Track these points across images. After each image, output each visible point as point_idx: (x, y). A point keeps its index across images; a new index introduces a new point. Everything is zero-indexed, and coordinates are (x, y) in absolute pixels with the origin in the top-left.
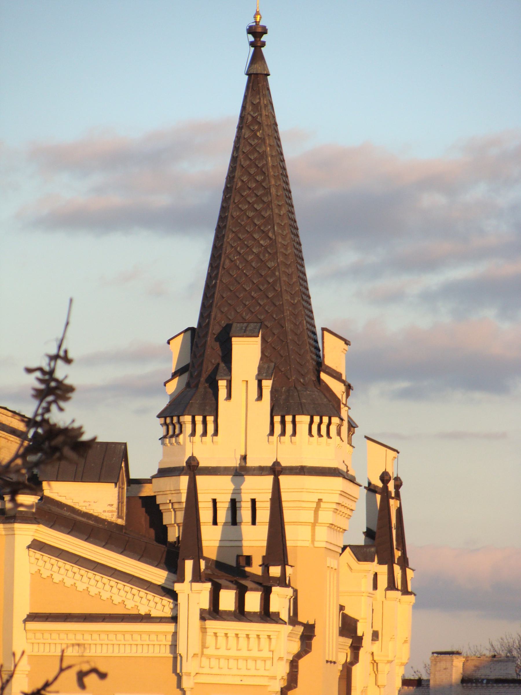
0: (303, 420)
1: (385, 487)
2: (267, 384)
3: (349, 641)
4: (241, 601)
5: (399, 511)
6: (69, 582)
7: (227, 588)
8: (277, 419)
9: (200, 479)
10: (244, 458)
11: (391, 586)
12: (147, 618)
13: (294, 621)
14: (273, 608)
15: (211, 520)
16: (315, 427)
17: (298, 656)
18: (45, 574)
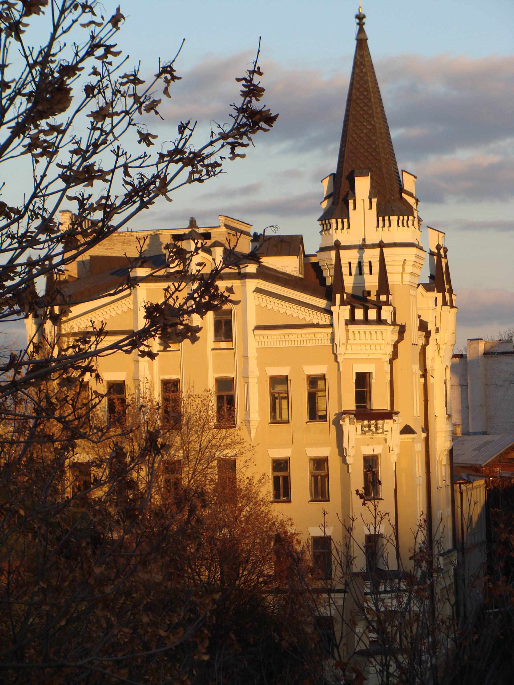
0: (394, 218)
1: (439, 252)
2: (374, 201)
3: (424, 334)
4: (366, 314)
5: (447, 265)
6: (276, 309)
8: (381, 219)
9: (342, 252)
10: (364, 240)
11: (445, 304)
12: (317, 326)
13: (394, 323)
14: (383, 317)
15: (348, 273)
16: (400, 222)
17: (398, 342)
18: (263, 305)
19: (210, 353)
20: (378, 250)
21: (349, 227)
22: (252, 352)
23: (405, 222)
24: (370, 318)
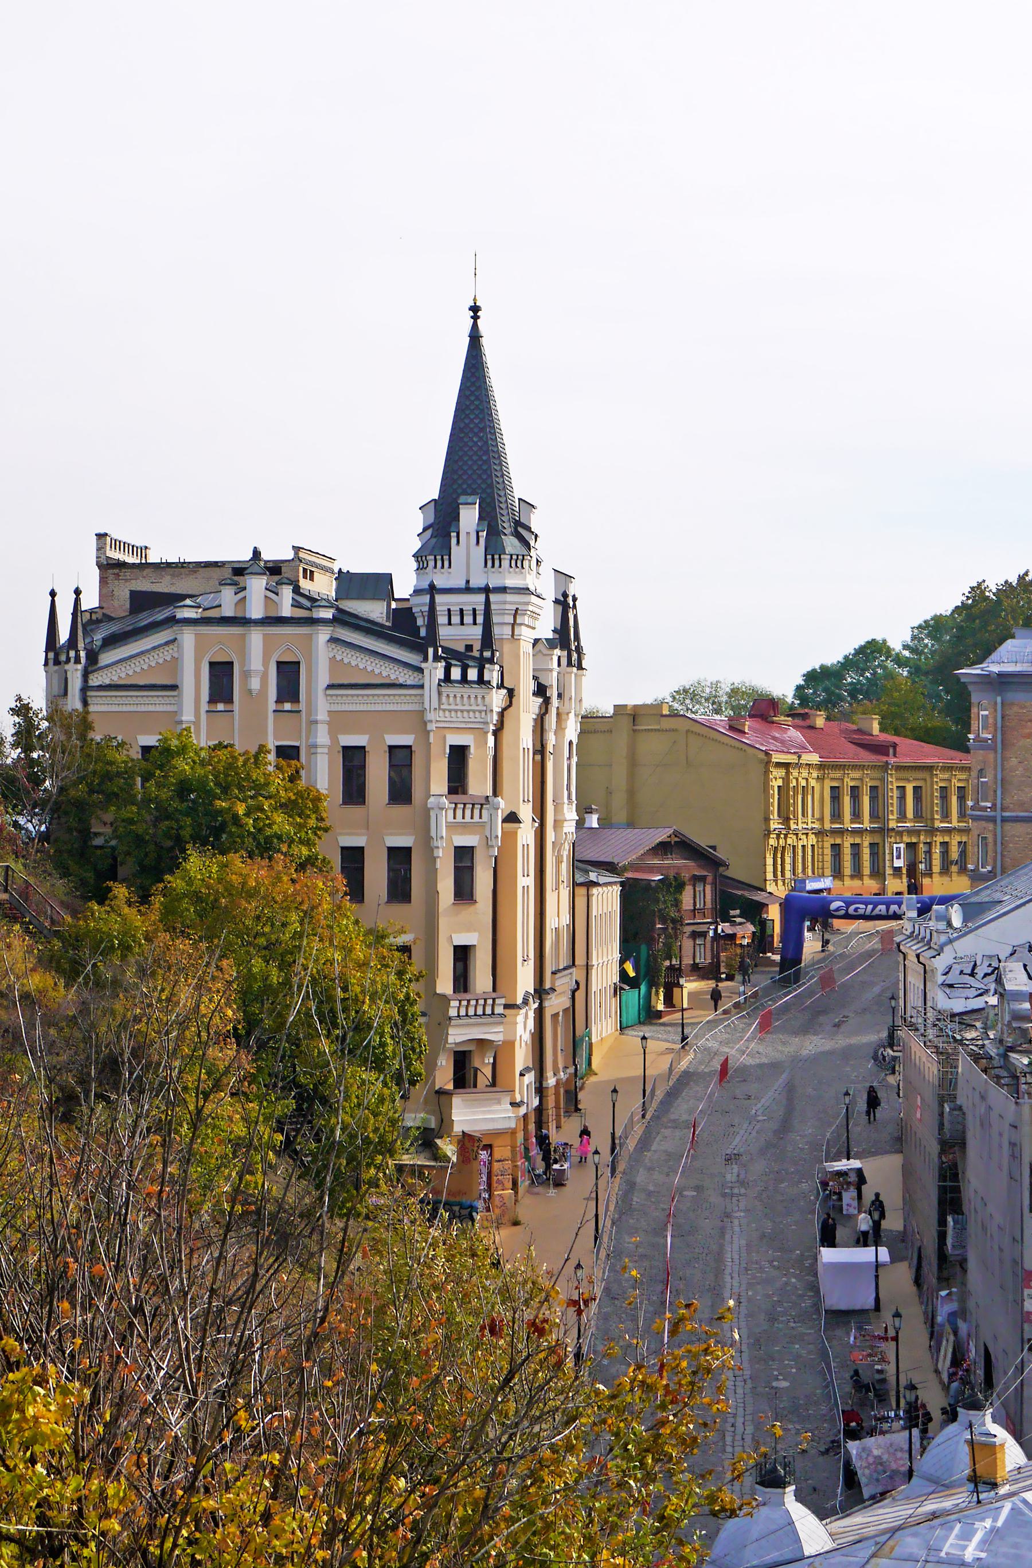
1: (565, 600)
3: (541, 700)
4: (464, 674)
5: (576, 617)
7: (456, 665)
8: (489, 557)
9: (439, 599)
10: (468, 582)
11: (570, 664)
12: (401, 686)
13: (501, 686)
14: (486, 678)
15: (446, 622)
16: (513, 563)
17: (504, 709)
18: (338, 658)
19: (271, 716)
20: (481, 598)
21: (450, 567)
22: (322, 716)
23: (519, 563)
24: (469, 678)
